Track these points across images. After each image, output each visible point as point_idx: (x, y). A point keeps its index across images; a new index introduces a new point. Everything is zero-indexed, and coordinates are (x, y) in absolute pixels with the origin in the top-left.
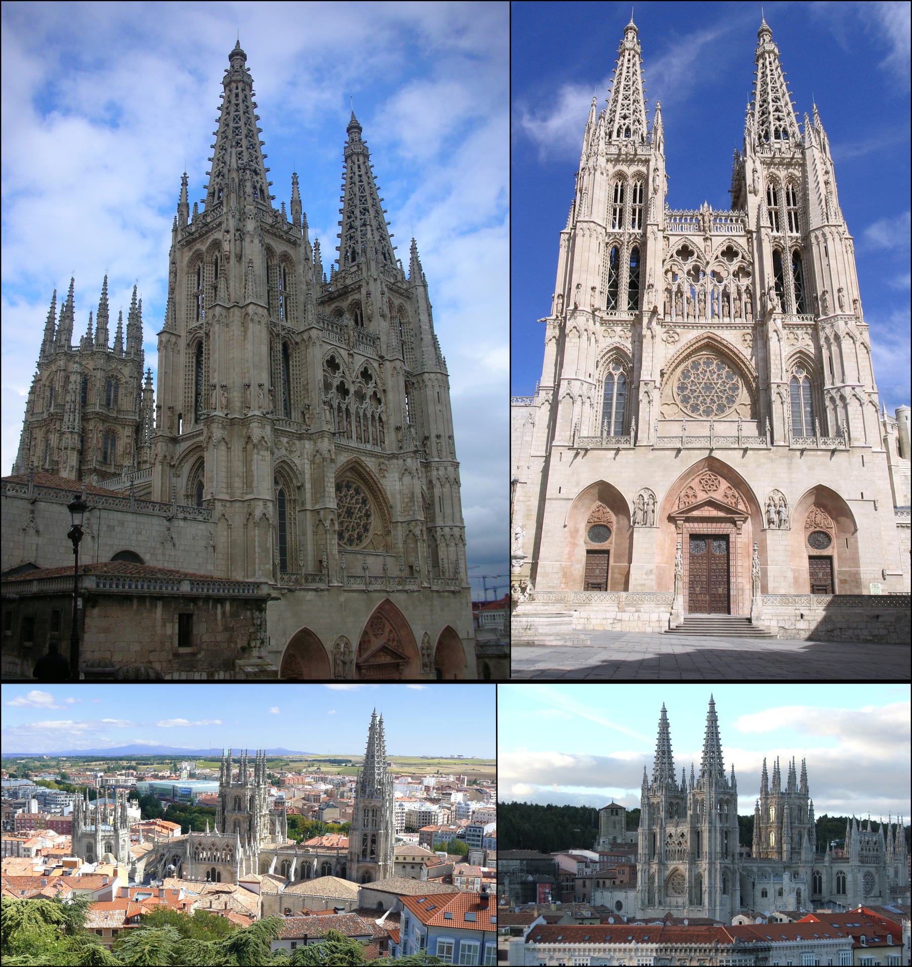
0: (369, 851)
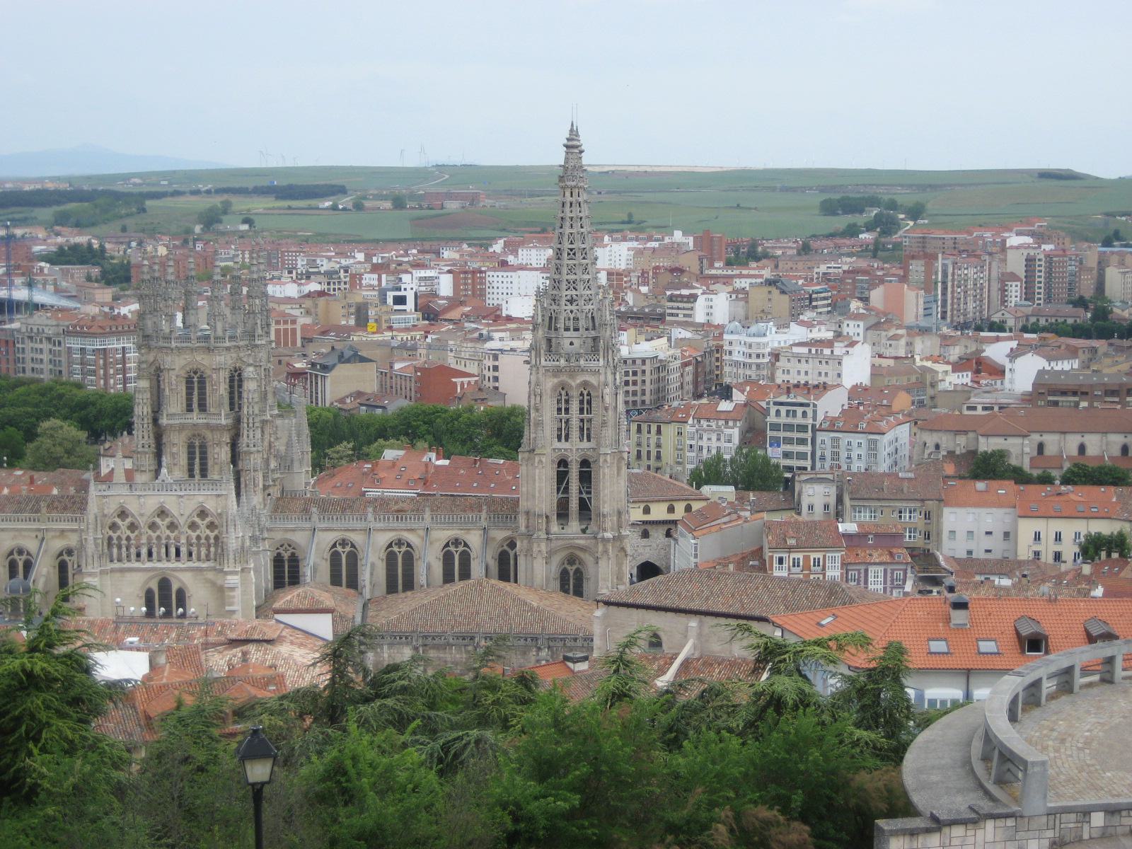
0: (574, 505)
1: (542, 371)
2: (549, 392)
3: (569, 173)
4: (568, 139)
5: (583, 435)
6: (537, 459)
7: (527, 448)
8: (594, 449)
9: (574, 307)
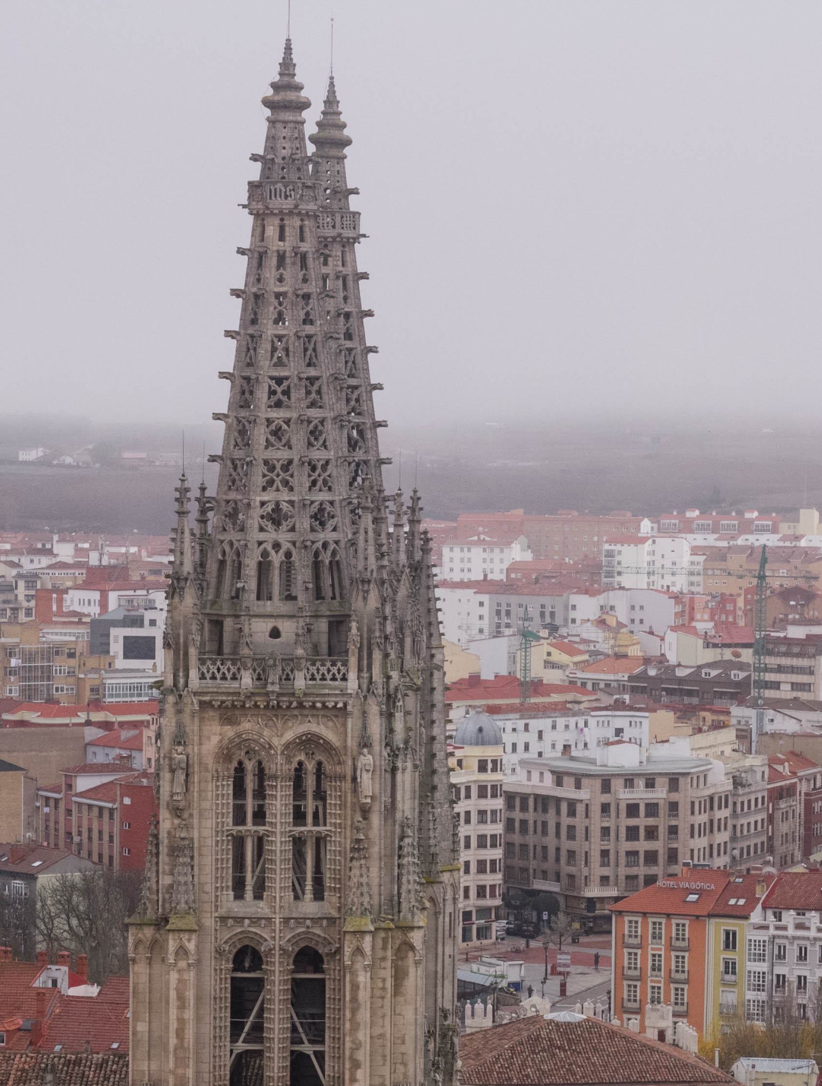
1: (192, 703)
2: (210, 761)
3: (276, 174)
4: (275, 86)
5: (301, 881)
6: (172, 945)
7: (150, 914)
8: (331, 920)
9: (284, 537)
